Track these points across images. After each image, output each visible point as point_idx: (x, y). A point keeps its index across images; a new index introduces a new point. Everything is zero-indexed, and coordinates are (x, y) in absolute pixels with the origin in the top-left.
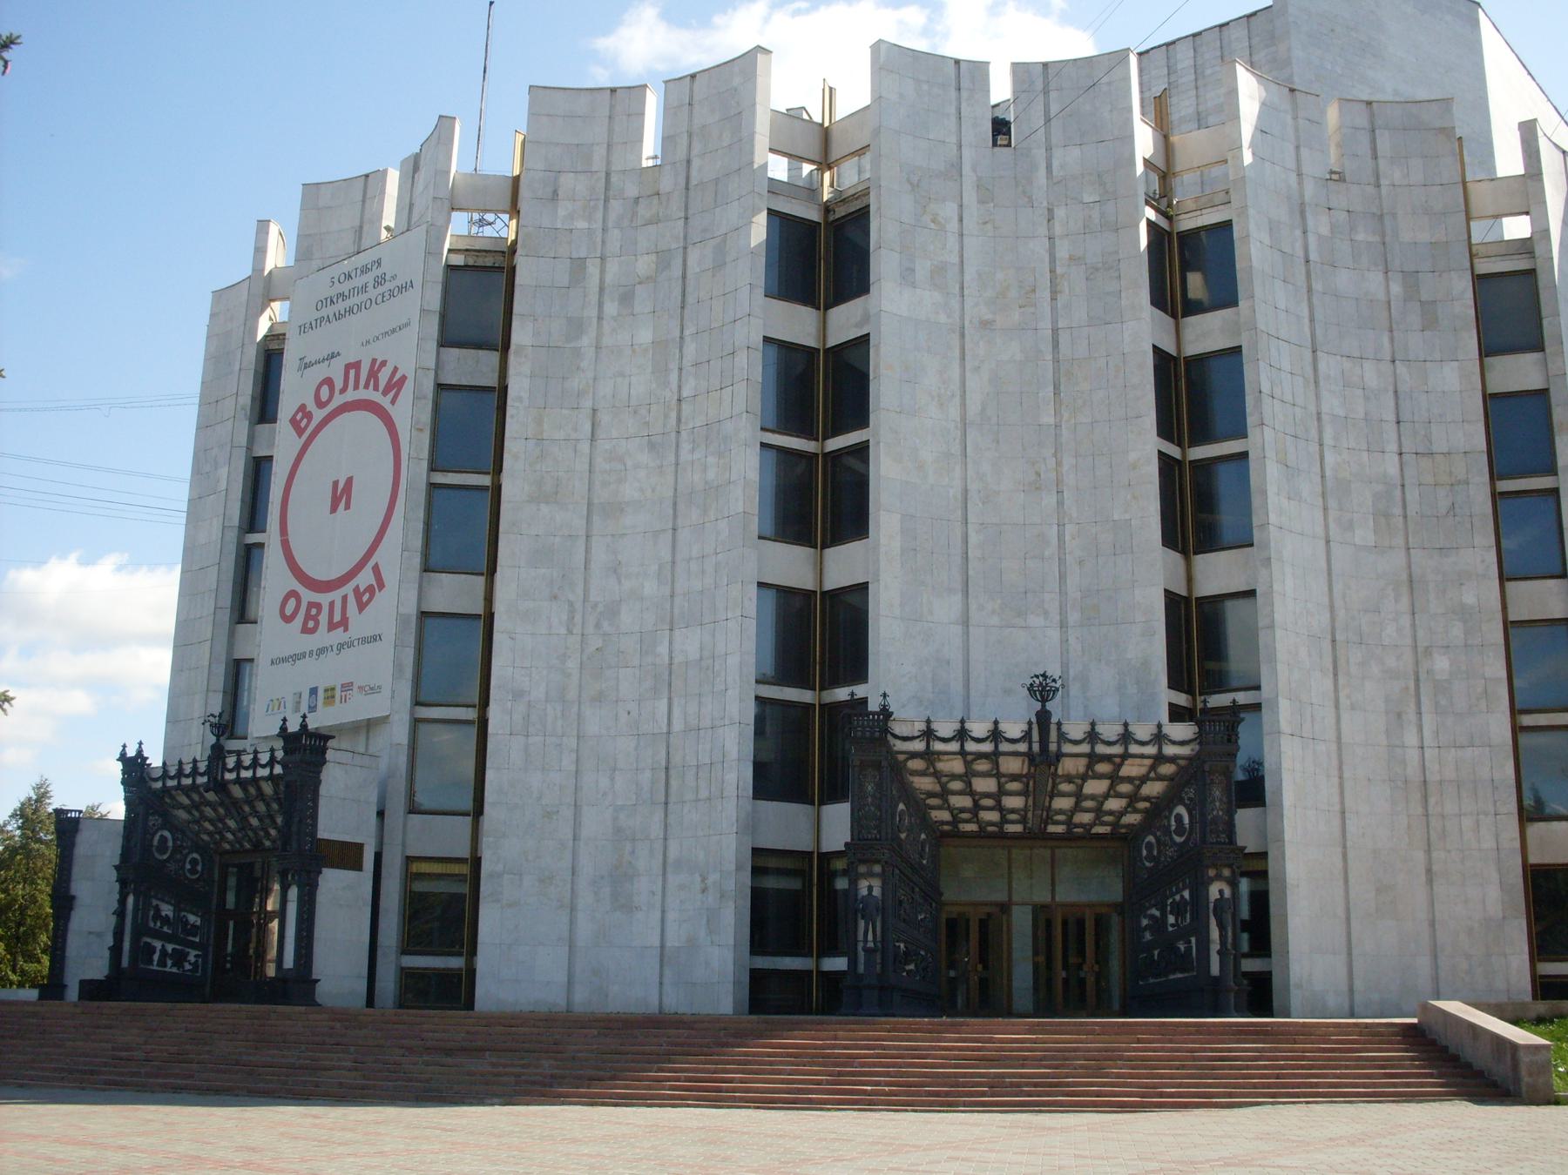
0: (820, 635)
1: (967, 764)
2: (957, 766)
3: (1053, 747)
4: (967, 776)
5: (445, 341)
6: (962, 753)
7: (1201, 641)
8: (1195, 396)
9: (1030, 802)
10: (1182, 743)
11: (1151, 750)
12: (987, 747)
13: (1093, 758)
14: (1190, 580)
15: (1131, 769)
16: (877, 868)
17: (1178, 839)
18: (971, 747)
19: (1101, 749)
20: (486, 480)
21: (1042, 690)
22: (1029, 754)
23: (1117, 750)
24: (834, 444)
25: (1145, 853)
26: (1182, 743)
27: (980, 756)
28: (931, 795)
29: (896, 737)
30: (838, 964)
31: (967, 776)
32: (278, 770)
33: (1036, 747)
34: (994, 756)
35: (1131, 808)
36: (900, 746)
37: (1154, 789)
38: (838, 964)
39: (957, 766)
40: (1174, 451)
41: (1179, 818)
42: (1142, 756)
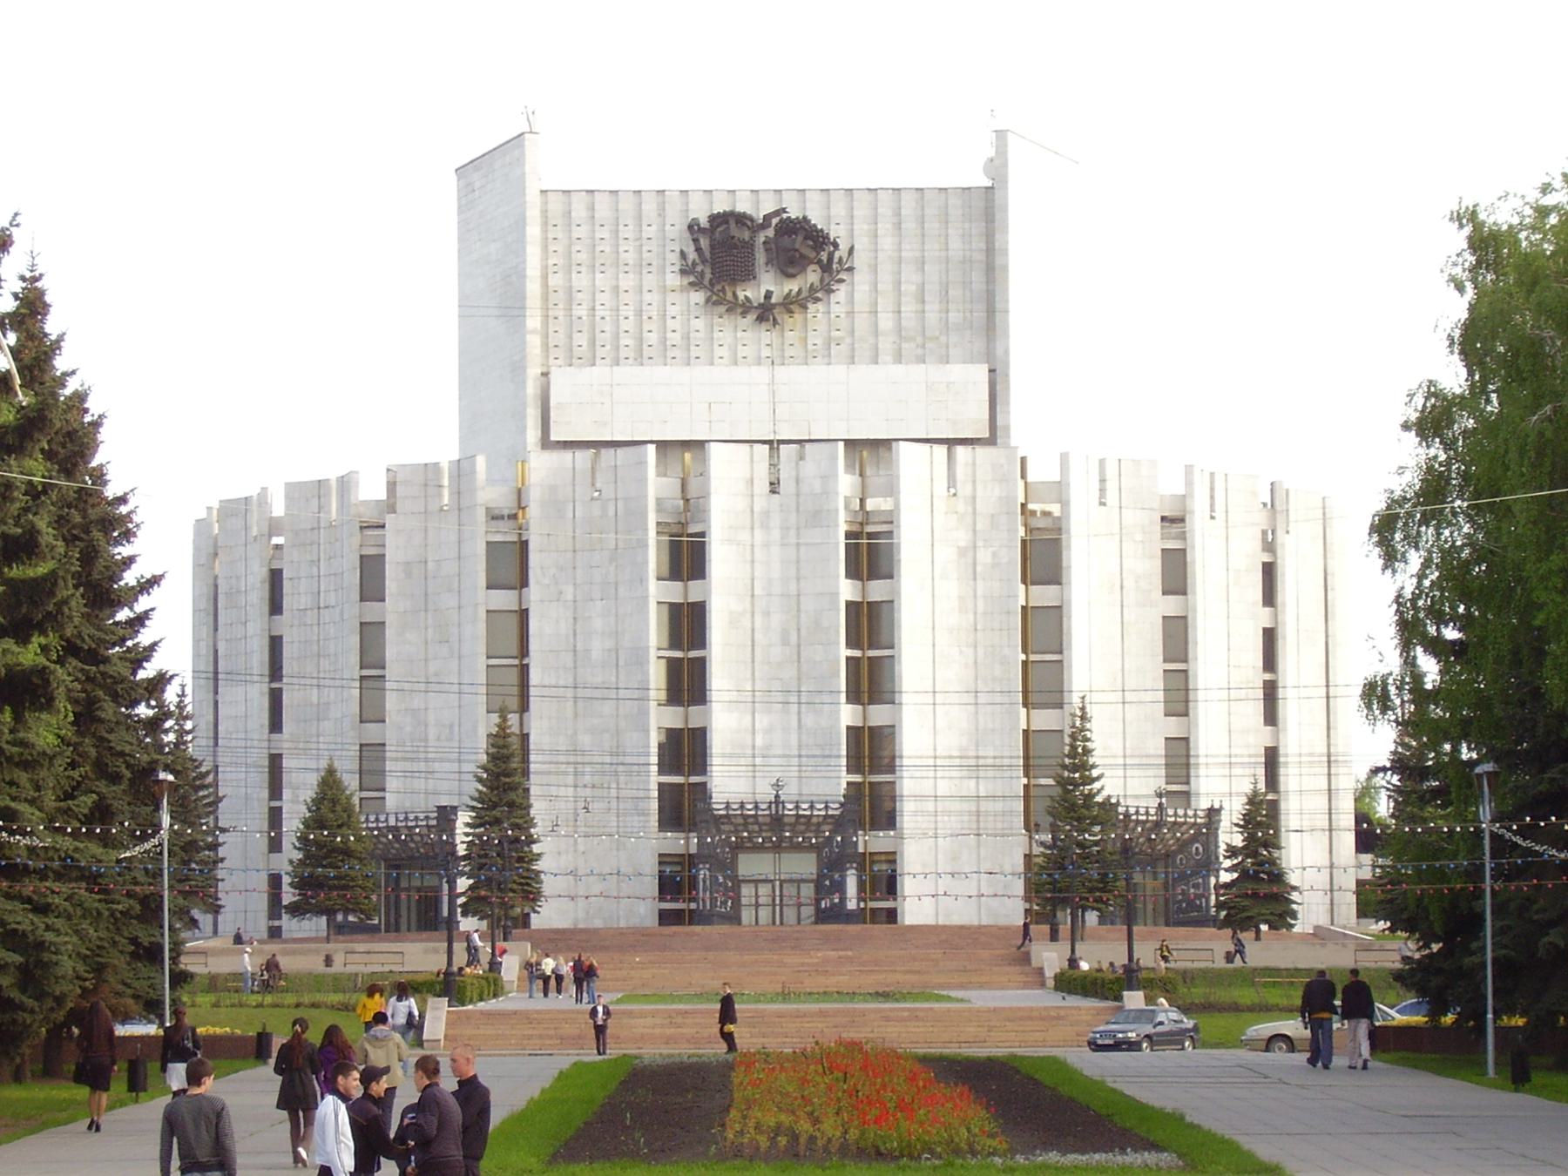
0: (686, 750)
2: (740, 821)
4: (746, 825)
5: (488, 588)
7: (871, 750)
8: (869, 624)
13: (798, 816)
14: (865, 719)
15: (814, 820)
20: (516, 662)
21: (777, 785)
24: (693, 654)
30: (693, 906)
31: (746, 825)
32: (434, 822)
34: (755, 816)
38: (693, 906)
39: (740, 821)
40: (857, 653)
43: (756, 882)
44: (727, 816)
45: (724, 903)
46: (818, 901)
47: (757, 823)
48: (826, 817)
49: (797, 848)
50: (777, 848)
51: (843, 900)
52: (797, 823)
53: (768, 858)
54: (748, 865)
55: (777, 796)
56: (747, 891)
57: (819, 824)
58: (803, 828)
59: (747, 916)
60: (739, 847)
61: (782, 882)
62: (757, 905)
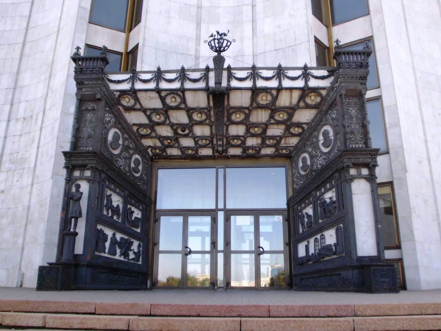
1: (163, 99)
2: (157, 104)
3: (224, 84)
6: (158, 91)
9: (214, 131)
10: (323, 78)
11: (300, 83)
12: (176, 85)
15: (284, 100)
16: (88, 173)
17: (325, 150)
18: (164, 85)
19: (260, 83)
21: (219, 45)
22: (207, 89)
23: (274, 84)
25: (301, 164)
26: (323, 78)
27: (172, 92)
28: (140, 126)
29: (111, 81)
31: (166, 109)
33: (212, 83)
35: (288, 133)
36: (113, 87)
37: (304, 116)
39: (157, 104)
41: (326, 134)
42: (291, 89)
43: (186, 214)
44: (133, 93)
45: (125, 246)
46: (292, 239)
47: (183, 106)
48: (306, 91)
49: (251, 158)
50: (220, 155)
51: (347, 236)
52: (255, 105)
53: (206, 176)
54: (175, 189)
55: (219, 60)
56: (168, 233)
57: (291, 110)
58: (261, 116)
59: (167, 267)
60: (157, 159)
61: (229, 214)
62: (187, 252)
